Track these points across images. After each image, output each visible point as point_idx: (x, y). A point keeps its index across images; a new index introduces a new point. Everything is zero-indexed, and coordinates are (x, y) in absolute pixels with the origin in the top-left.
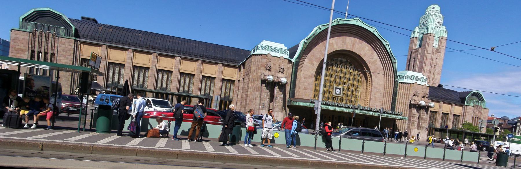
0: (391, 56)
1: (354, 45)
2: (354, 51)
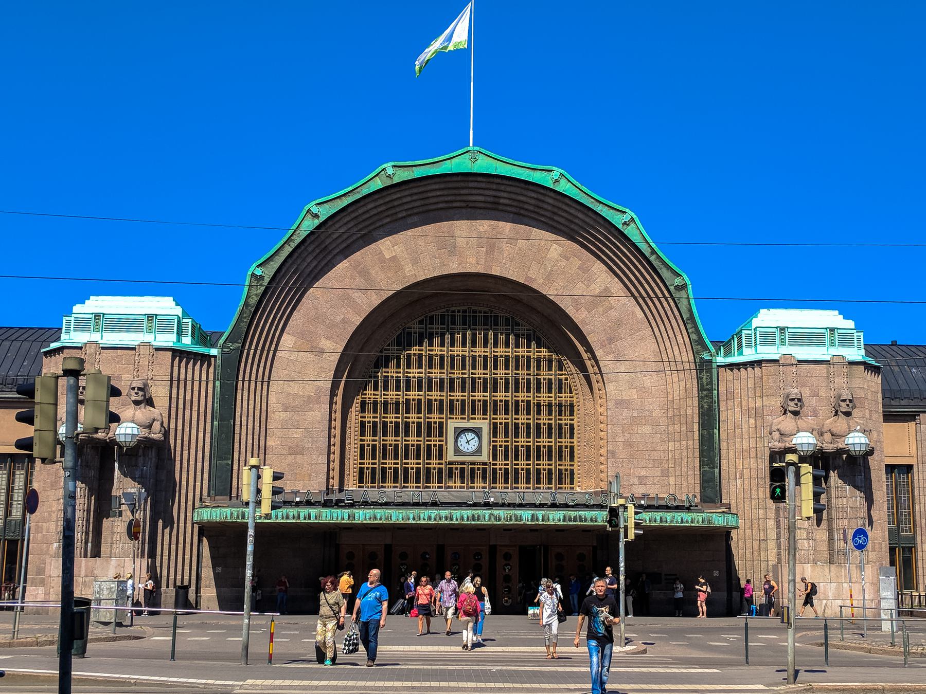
0: (656, 263)
1: (490, 250)
2: (496, 271)
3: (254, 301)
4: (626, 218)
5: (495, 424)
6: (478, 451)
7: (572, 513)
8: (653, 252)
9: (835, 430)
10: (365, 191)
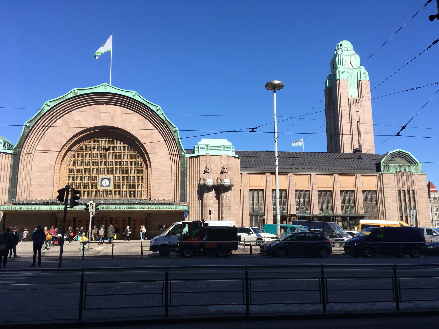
0: (167, 123)
1: (113, 118)
2: (114, 125)
3: (26, 134)
4: (158, 108)
5: (115, 177)
6: (109, 186)
7: (129, 206)
8: (166, 120)
9: (221, 178)
10: (67, 98)
